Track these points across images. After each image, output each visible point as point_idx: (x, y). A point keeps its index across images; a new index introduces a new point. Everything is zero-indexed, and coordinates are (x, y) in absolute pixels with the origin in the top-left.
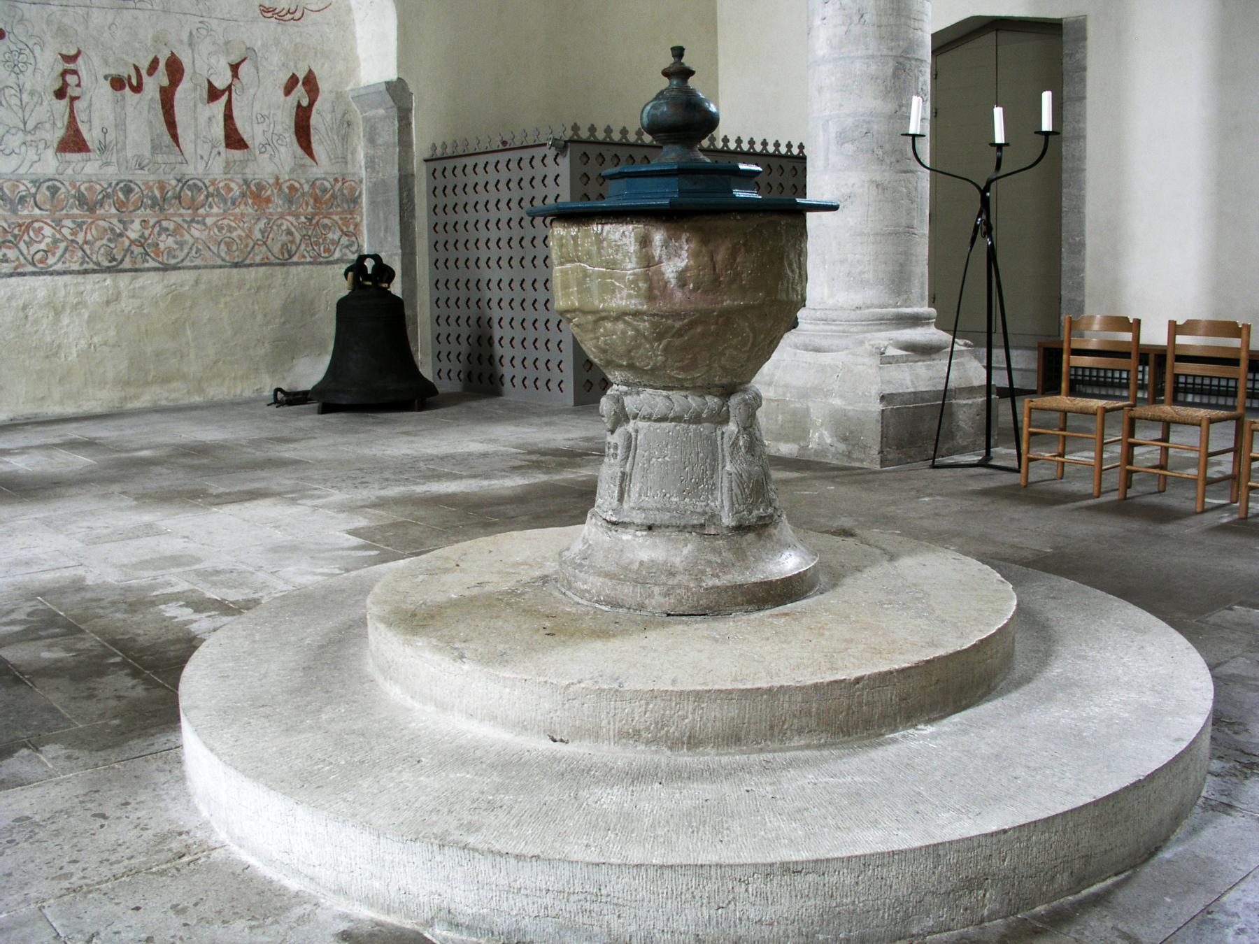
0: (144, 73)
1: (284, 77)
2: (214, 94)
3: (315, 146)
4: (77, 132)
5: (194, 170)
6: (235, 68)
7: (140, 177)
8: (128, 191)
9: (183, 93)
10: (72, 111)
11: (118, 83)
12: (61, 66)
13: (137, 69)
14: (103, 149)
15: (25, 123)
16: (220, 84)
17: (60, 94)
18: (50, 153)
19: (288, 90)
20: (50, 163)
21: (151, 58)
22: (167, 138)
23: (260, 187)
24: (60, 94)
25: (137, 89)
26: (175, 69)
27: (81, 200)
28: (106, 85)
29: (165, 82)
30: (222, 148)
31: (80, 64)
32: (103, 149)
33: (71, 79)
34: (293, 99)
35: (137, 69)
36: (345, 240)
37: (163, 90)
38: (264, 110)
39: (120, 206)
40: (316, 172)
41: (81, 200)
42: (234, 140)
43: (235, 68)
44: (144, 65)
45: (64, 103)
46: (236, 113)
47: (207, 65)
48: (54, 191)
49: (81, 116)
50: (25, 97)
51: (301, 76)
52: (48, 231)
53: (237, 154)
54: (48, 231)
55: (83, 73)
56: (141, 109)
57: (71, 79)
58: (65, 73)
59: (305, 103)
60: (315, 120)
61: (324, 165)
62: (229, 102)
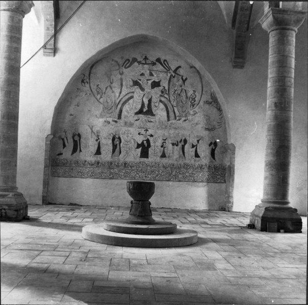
1: (209, 142)
2: (193, 146)
3: (216, 157)
4: (165, 154)
5: (187, 161)
6: (198, 141)
7: (175, 163)
8: (173, 165)
9: (186, 146)
11: (173, 144)
12: (163, 141)
14: (169, 157)
16: (194, 144)
17: (162, 146)
18: (158, 158)
19: (210, 145)
20: (158, 159)
22: (182, 155)
23: (202, 166)
25: (177, 145)
26: (185, 141)
27: (164, 167)
28: (171, 145)
30: (194, 157)
31: (167, 141)
32: (169, 157)
33: (164, 144)
34: (211, 147)
36: (221, 178)
37: (182, 145)
38: (204, 150)
39: (171, 168)
40: (216, 163)
41: (164, 167)
42: (197, 155)
43: (198, 141)
45: (163, 148)
46: (198, 150)
47: (192, 140)
48: (159, 165)
49: (166, 151)
51: (213, 142)
52: (157, 172)
53: (197, 159)
54: (157, 172)
56: (177, 149)
57: (164, 144)
58: (163, 143)
59: (214, 148)
60: (216, 152)
61: (217, 162)
62: (196, 148)
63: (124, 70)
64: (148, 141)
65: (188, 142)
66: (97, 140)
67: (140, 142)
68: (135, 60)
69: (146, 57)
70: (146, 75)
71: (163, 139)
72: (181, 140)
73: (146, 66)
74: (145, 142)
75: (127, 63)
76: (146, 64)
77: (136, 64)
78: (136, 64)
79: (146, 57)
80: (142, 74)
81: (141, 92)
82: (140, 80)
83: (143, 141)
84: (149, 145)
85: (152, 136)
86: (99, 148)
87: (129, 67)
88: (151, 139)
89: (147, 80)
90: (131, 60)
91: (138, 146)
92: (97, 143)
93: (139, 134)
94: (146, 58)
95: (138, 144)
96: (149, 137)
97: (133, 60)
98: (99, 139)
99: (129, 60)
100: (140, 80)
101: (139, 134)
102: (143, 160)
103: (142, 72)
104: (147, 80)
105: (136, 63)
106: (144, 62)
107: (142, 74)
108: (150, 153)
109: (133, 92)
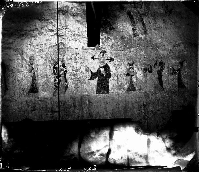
0: (153, 67)
4: (133, 85)
9: (165, 72)
10: (131, 79)
12: (128, 67)
13: (150, 66)
15: (118, 84)
17: (128, 75)
21: (155, 62)
22: (159, 86)
24: (128, 75)
25: (150, 72)
29: (159, 69)
33: (131, 70)
35: (150, 66)
37: (158, 71)
44: (153, 65)
50: (119, 76)
55: (135, 69)
57: (131, 70)
58: (130, 69)
64: (107, 68)
65: (166, 65)
66: (30, 71)
67: (95, 71)
71: (129, 64)
72: (156, 64)
74: (102, 70)
83: (100, 67)
84: (109, 75)
85: (112, 60)
86: (76, 49)
88: (111, 65)
91: (93, 76)
92: (30, 75)
93: (93, 58)
95: (92, 72)
96: (107, 62)
98: (33, 69)
101: (93, 58)
102: (102, 95)
108: (110, 86)
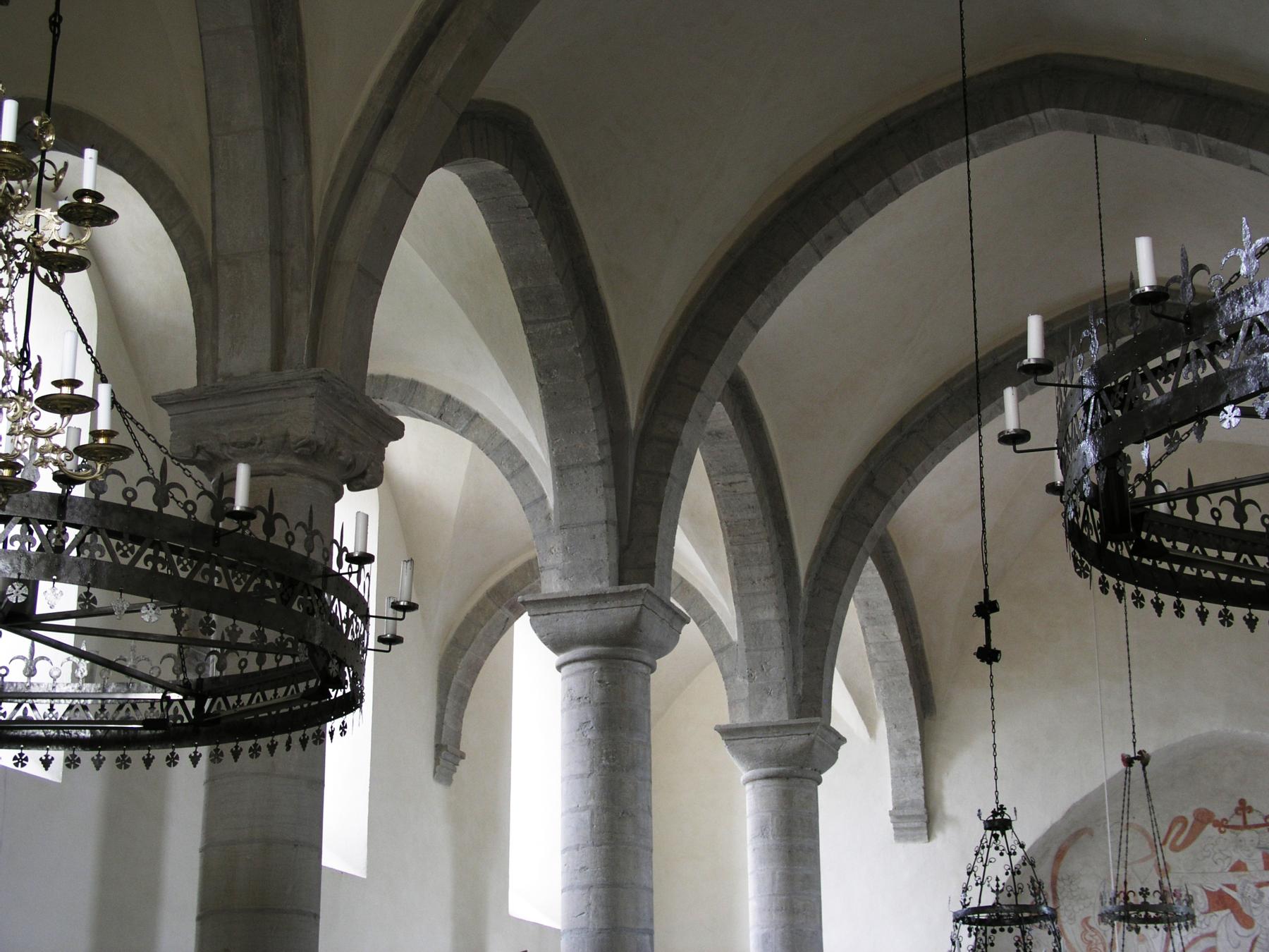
63: (1171, 857)
68: (1203, 818)
69: (1242, 802)
70: (1250, 867)
73: (1246, 834)
75: (1179, 834)
76: (1246, 826)
77: (1210, 830)
78: (1210, 830)
79: (1242, 802)
80: (1238, 867)
81: (1243, 931)
82: (1233, 887)
87: (1186, 843)
89: (1259, 885)
90: (1191, 820)
94: (1243, 808)
97: (1196, 819)
99: (1183, 820)
100: (1233, 887)
103: (1236, 857)
104: (1259, 885)
105: (1209, 827)
106: (1238, 821)
107: (1238, 867)
109: (1214, 935)
